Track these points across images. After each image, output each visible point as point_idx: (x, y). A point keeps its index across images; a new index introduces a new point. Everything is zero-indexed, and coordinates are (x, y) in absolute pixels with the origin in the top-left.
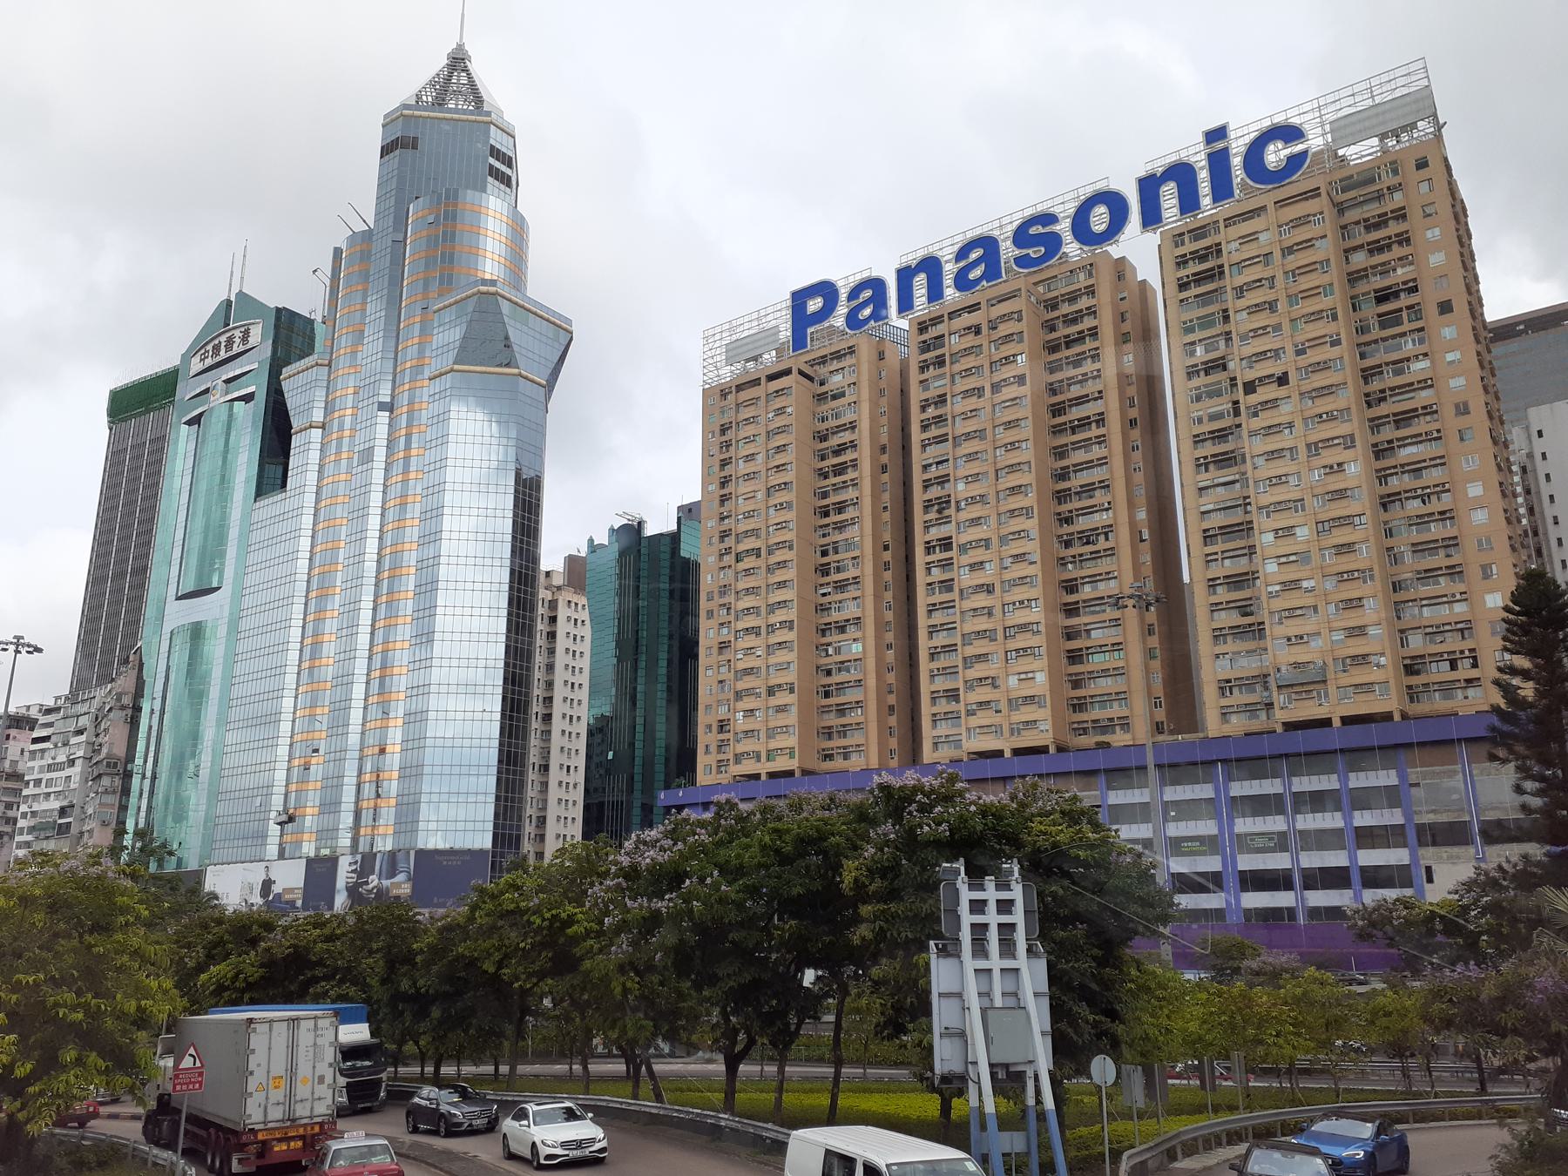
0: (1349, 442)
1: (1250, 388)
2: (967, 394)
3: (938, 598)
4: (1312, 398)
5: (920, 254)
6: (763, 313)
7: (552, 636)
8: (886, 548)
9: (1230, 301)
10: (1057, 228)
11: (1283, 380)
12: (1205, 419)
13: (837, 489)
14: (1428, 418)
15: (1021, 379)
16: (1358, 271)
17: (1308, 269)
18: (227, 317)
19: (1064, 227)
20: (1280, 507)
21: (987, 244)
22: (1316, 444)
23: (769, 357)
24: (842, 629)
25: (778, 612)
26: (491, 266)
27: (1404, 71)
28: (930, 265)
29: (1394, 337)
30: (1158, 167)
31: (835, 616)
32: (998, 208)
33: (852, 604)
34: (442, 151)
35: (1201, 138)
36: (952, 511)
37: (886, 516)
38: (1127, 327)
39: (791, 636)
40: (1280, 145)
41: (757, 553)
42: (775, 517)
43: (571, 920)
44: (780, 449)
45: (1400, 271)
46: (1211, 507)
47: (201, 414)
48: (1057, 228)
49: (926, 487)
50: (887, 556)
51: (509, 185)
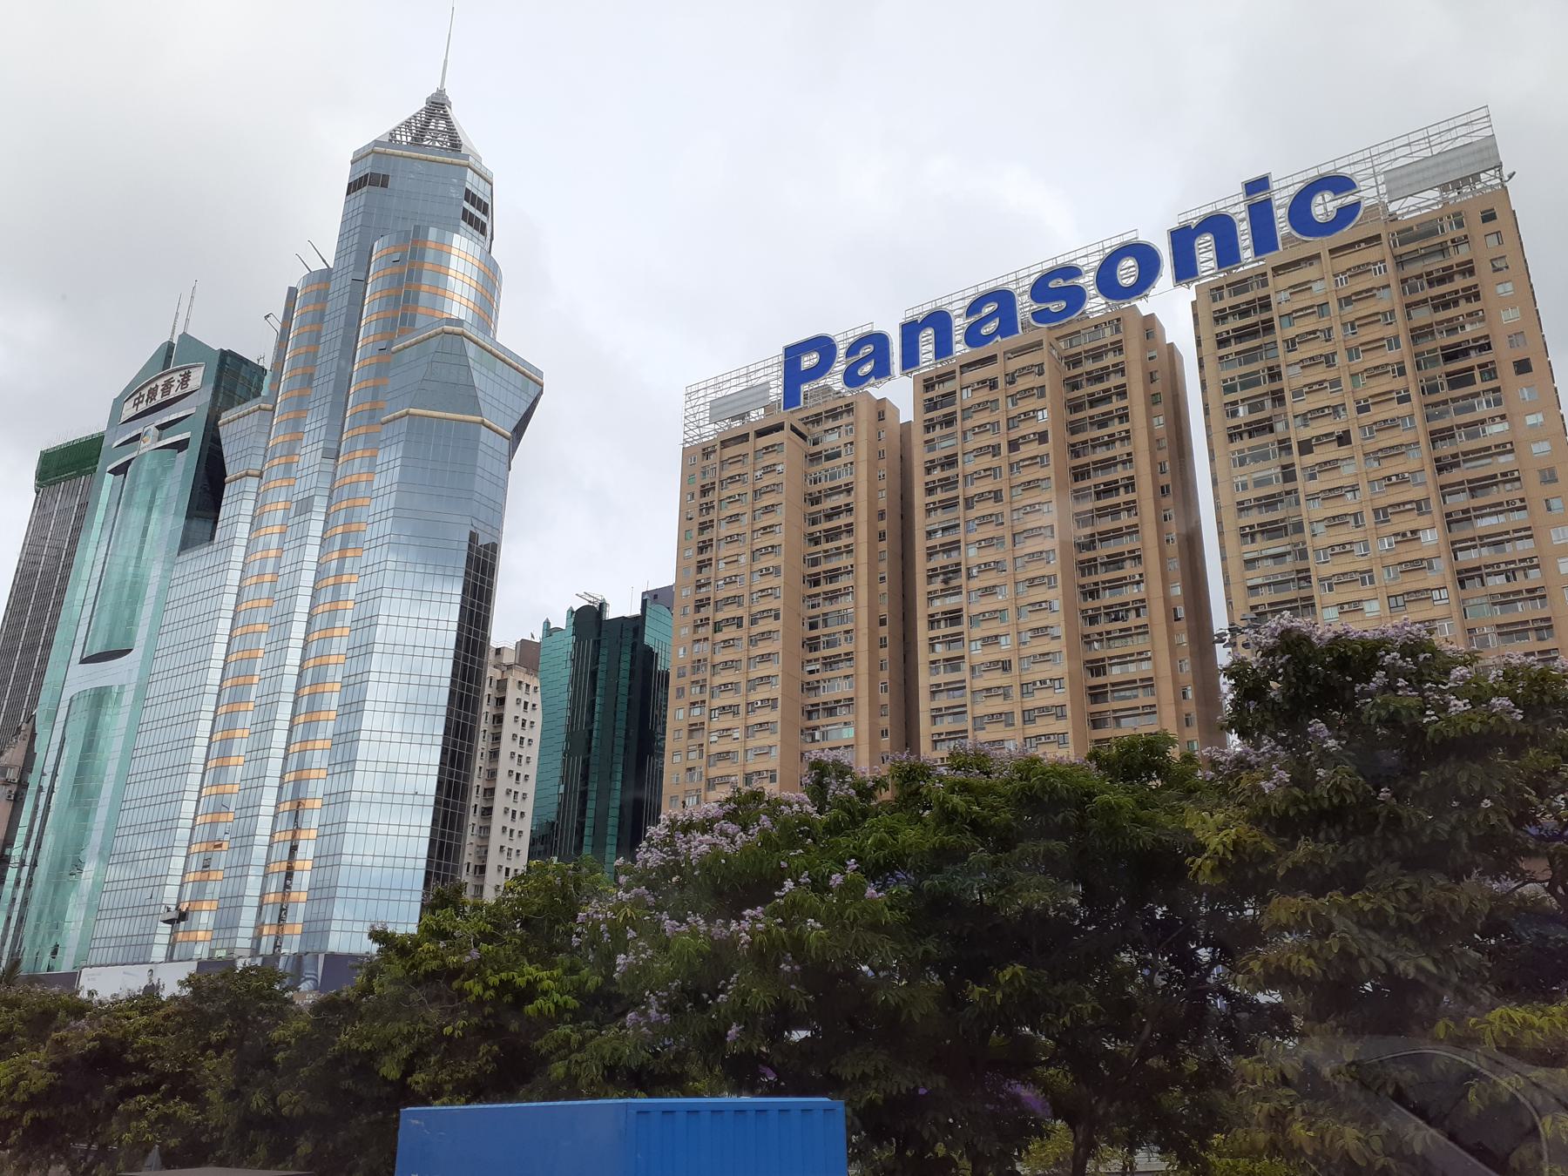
0: (1420, 506)
1: (1306, 447)
2: (980, 451)
3: (943, 677)
4: (1378, 459)
5: (928, 308)
6: (752, 369)
7: (498, 719)
8: (883, 623)
9: (1283, 357)
10: (1080, 281)
11: (1343, 439)
12: (1251, 485)
13: (828, 555)
14: (1508, 486)
15: (1042, 437)
16: (1421, 328)
17: (1369, 320)
18: (169, 357)
19: (1087, 281)
20: (1345, 579)
21: (1003, 298)
22: (1384, 509)
23: (757, 415)
24: (831, 711)
25: (759, 689)
26: (459, 303)
27: (1464, 120)
28: (939, 320)
29: (1465, 398)
30: (1193, 217)
31: (824, 696)
32: (1015, 265)
33: (844, 684)
34: (416, 187)
35: (1240, 189)
36: (962, 580)
37: (884, 587)
38: (1156, 387)
39: (773, 716)
40: (1328, 196)
41: (739, 622)
42: (761, 583)
43: (530, 992)
44: (769, 509)
45: (1468, 328)
46: (1259, 581)
47: (129, 462)
48: (1080, 281)
49: (930, 555)
50: (884, 631)
51: (483, 232)
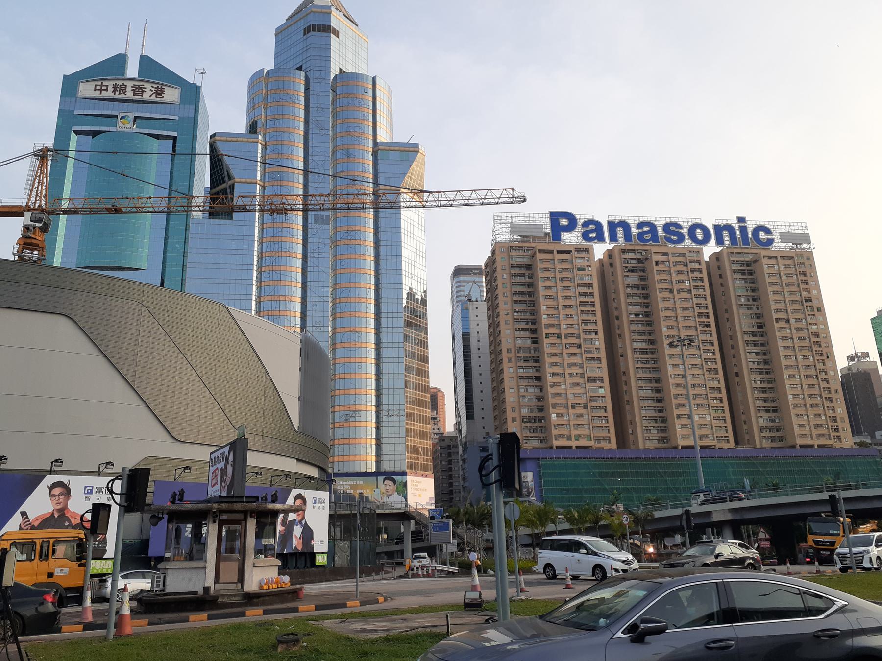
21: (653, 227)
